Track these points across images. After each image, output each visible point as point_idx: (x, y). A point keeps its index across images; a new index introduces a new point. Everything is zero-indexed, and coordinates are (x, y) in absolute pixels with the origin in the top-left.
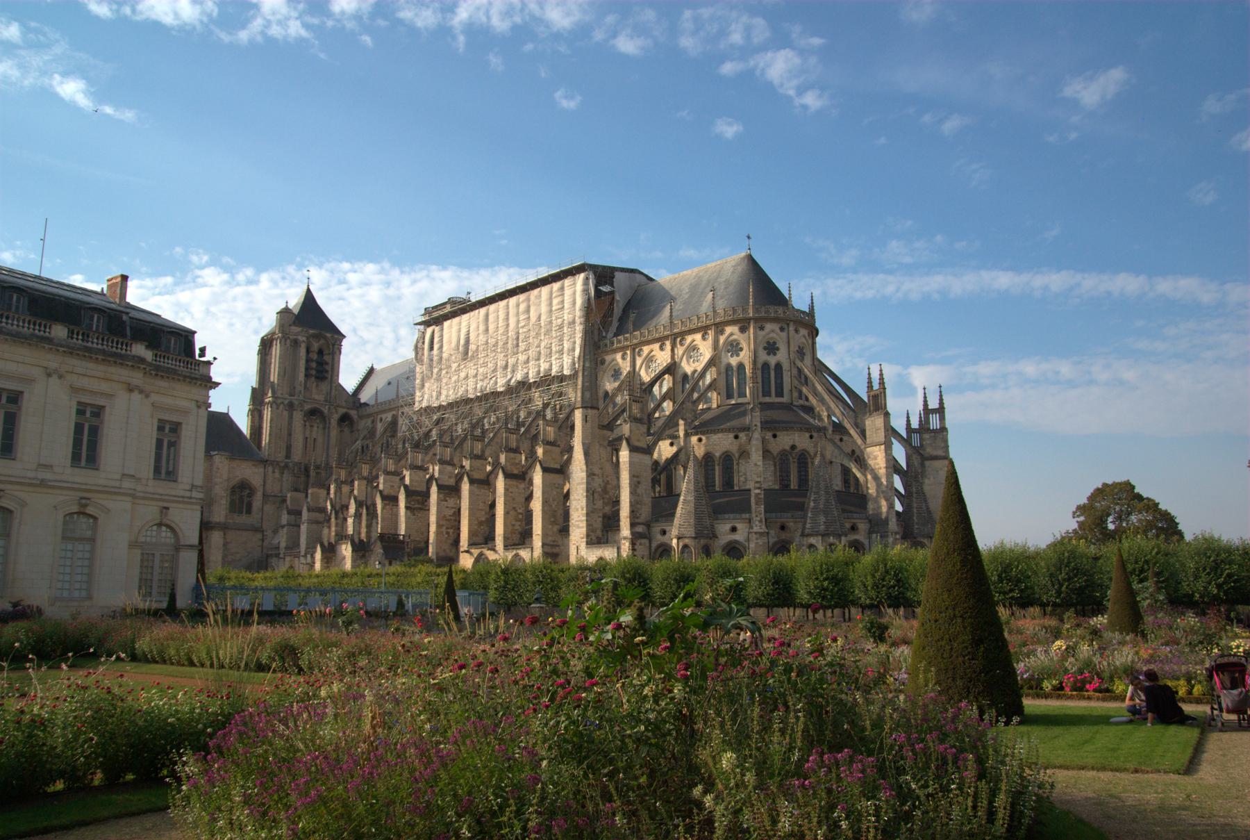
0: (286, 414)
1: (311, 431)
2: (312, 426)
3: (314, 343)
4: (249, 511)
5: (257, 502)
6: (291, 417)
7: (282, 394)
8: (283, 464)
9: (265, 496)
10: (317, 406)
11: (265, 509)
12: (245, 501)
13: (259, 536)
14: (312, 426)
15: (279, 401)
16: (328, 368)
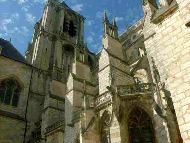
0: (50, 42)
1: (67, 60)
2: (67, 57)
3: (69, 17)
4: (15, 104)
5: (23, 96)
6: (53, 47)
7: (48, 31)
8: (46, 73)
9: (30, 92)
10: (70, 44)
11: (29, 103)
12: (13, 95)
13: (23, 125)
14: (67, 57)
15: (46, 34)
16: (77, 30)
